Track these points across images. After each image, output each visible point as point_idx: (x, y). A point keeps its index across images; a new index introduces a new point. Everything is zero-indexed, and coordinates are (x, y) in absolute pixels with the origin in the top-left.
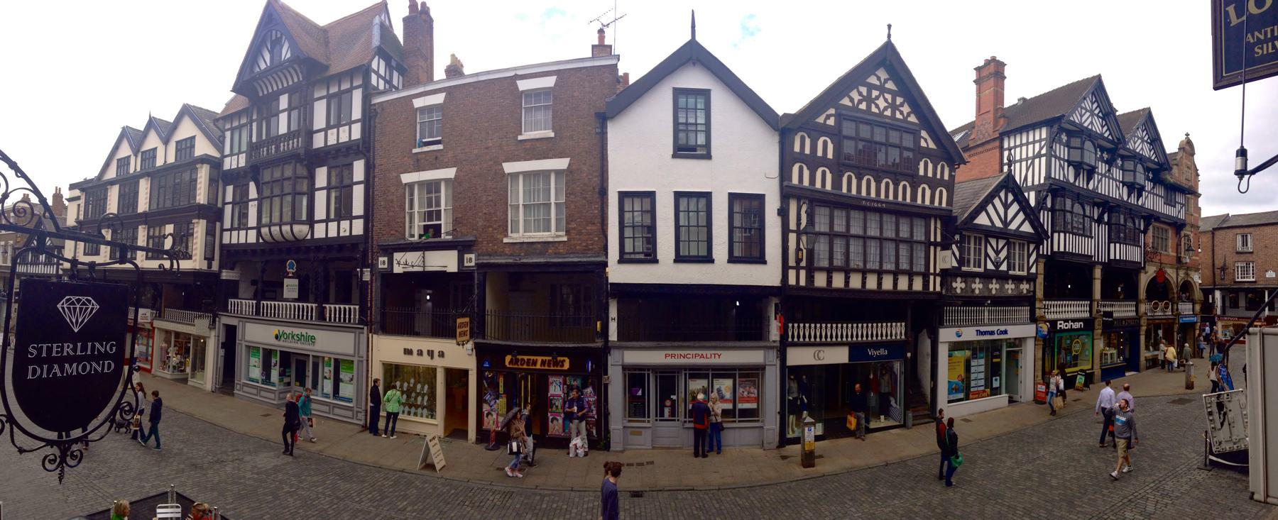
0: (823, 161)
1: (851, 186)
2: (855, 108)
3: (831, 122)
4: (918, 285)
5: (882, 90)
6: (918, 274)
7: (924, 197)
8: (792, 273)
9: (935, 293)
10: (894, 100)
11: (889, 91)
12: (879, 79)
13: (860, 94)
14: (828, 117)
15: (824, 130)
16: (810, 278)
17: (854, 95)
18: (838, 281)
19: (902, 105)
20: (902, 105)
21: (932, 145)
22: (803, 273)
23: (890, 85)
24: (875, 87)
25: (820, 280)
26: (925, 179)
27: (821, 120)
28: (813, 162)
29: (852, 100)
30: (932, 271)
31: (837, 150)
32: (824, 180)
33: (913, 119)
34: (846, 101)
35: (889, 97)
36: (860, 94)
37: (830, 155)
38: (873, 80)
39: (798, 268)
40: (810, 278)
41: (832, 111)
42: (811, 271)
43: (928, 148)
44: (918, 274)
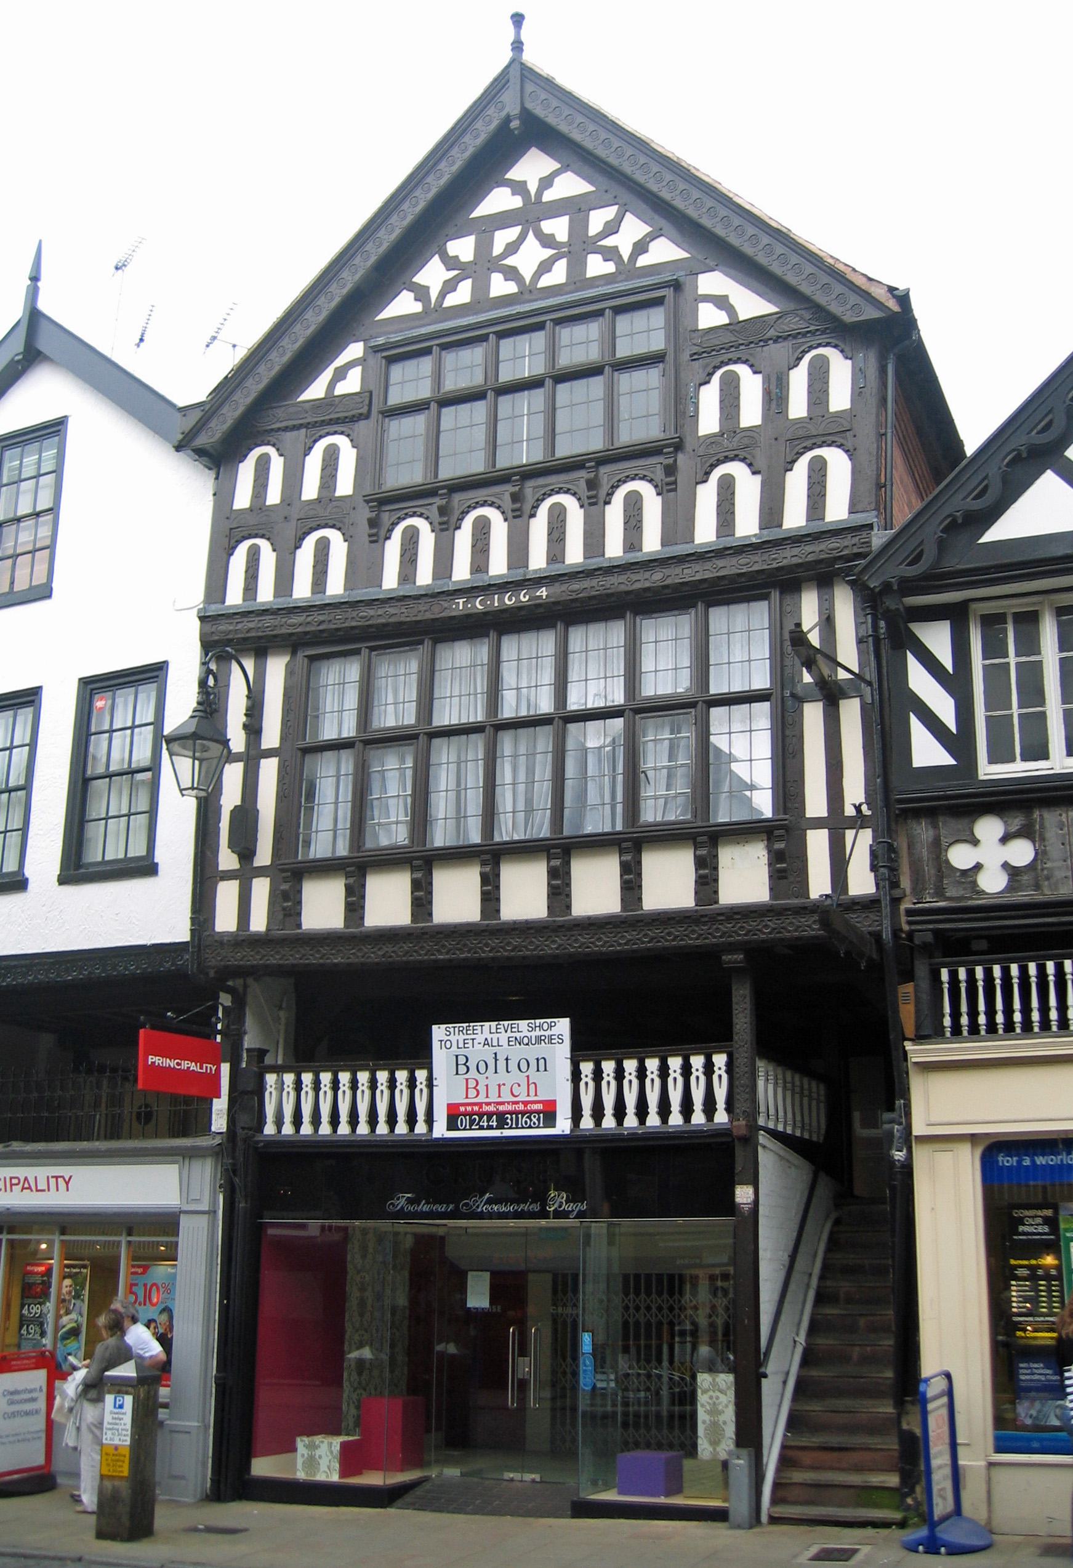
0: (328, 511)
1: (416, 560)
2: (433, 311)
3: (352, 384)
4: (745, 878)
5: (531, 215)
6: (745, 831)
7: (731, 507)
8: (227, 894)
9: (842, 904)
10: (578, 226)
11: (557, 209)
12: (519, 188)
13: (451, 262)
14: (340, 374)
15: (336, 416)
16: (287, 904)
17: (432, 274)
18: (388, 902)
19: (612, 228)
20: (612, 228)
21: (751, 305)
22: (261, 888)
23: (571, 185)
24: (503, 220)
25: (322, 907)
26: (734, 444)
27: (316, 391)
28: (286, 524)
29: (421, 293)
30: (816, 804)
31: (370, 464)
32: (321, 569)
33: (665, 251)
34: (404, 304)
35: (558, 227)
36: (451, 262)
37: (345, 486)
38: (498, 200)
39: (245, 875)
40: (287, 904)
41: (355, 350)
42: (292, 875)
43: (735, 326)
44: (745, 831)
